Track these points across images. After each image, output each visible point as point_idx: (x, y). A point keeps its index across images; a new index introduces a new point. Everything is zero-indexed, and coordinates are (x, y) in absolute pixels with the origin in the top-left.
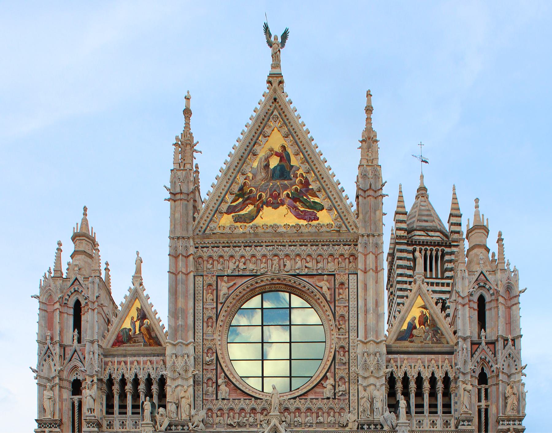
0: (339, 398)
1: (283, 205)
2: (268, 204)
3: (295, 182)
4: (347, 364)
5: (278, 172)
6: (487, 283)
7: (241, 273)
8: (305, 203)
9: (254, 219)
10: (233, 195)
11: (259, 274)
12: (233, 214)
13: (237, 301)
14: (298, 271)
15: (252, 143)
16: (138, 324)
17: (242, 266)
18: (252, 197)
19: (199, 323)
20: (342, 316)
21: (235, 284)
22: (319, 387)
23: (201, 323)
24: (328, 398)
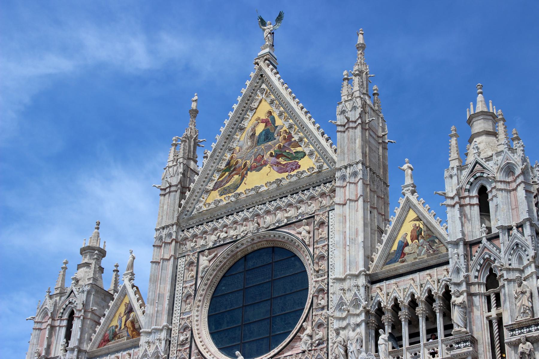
0: (316, 348)
1: (265, 164)
2: (251, 169)
3: (279, 140)
4: (326, 307)
5: (263, 137)
6: (485, 171)
7: (222, 243)
8: (288, 156)
9: (238, 187)
10: (220, 172)
11: (238, 238)
12: (219, 189)
13: (219, 271)
14: (277, 224)
15: (239, 120)
16: (124, 319)
17: (223, 235)
18: (238, 167)
19: (178, 304)
20: (322, 257)
21: (216, 255)
22: (296, 340)
23: (179, 303)
24: (304, 352)
